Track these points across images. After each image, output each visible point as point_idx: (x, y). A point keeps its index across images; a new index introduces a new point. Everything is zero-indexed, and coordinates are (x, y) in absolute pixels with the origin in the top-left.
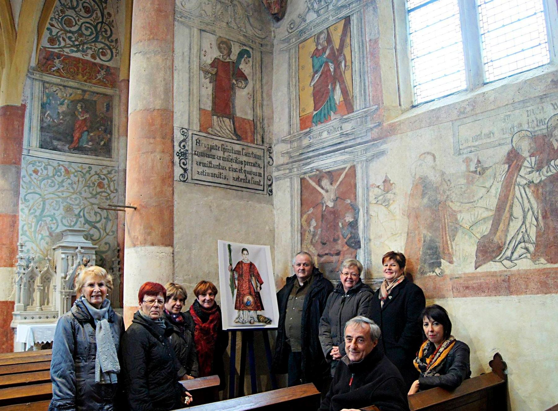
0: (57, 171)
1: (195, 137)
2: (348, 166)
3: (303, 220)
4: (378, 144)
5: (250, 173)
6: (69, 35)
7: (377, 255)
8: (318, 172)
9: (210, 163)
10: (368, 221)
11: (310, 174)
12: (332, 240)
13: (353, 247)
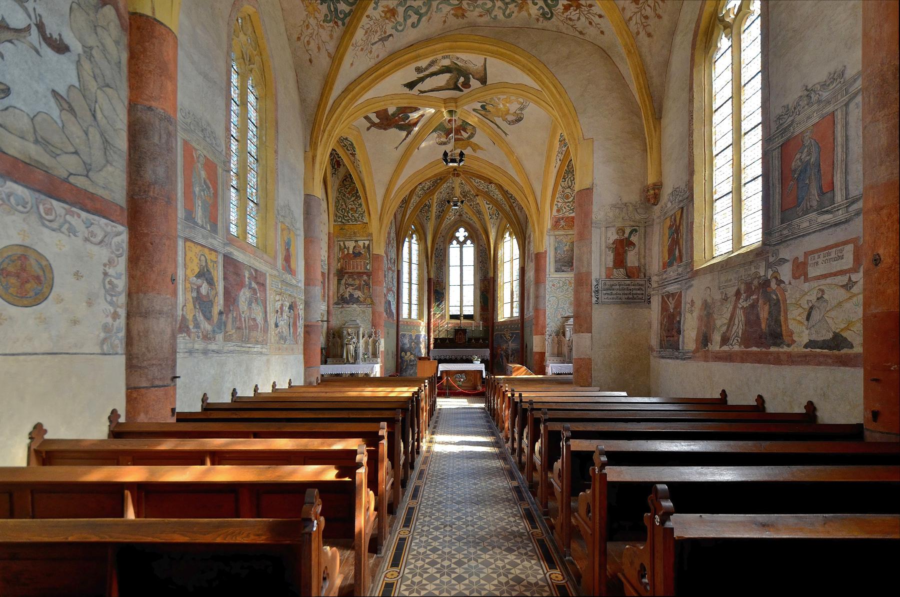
0: (564, 283)
1: (603, 282)
2: (679, 291)
5: (636, 294)
6: (567, 204)
9: (612, 293)
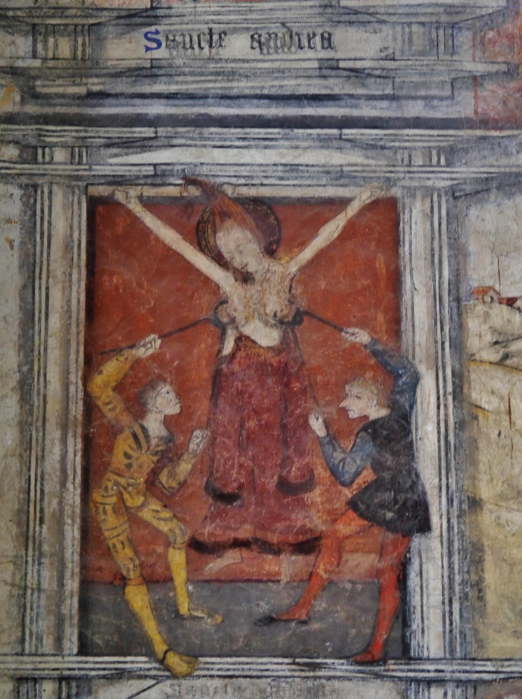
3: (98, 380)
4: (506, 142)
7: (512, 565)
8: (194, 191)
10: (461, 425)
11: (150, 192)
12: (271, 483)
13: (389, 525)
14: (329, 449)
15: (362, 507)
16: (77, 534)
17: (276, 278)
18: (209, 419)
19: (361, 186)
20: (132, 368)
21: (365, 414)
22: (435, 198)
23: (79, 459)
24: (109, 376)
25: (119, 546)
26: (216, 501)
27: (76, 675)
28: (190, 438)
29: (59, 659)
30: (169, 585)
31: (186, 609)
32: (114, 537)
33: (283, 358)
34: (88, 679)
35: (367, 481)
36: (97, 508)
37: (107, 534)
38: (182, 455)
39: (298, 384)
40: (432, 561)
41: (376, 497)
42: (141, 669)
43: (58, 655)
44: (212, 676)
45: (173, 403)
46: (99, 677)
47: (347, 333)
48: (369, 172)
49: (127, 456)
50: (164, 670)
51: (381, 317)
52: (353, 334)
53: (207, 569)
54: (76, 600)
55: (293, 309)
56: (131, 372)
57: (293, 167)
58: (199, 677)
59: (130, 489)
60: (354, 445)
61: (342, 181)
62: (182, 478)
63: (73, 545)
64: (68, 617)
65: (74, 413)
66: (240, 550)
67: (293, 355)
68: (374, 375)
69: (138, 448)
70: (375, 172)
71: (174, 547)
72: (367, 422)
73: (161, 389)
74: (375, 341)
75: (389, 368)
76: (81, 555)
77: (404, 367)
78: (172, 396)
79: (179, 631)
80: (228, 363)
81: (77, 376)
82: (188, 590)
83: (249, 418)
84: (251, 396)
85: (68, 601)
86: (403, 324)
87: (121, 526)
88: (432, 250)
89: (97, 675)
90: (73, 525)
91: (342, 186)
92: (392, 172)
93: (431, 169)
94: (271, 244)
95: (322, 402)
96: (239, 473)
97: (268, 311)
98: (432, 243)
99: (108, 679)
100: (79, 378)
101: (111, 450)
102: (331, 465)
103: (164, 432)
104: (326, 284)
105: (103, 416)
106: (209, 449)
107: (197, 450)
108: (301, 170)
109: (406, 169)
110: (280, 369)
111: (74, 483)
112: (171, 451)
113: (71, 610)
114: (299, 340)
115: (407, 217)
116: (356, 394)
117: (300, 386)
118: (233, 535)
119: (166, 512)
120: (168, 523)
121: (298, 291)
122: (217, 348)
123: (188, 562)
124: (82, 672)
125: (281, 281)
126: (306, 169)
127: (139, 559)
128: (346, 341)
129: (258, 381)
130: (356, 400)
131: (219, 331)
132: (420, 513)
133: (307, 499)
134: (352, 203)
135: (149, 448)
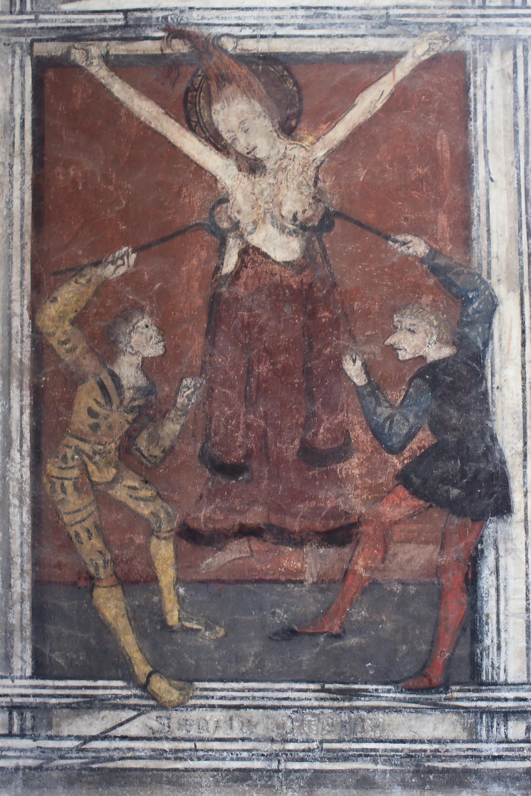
14: (371, 403)
15: (417, 481)
16: (27, 519)
17: (296, 167)
18: (204, 362)
19: (415, 36)
20: (96, 293)
21: (421, 353)
22: (520, 52)
23: (26, 417)
24: (65, 305)
25: (84, 535)
26: (214, 474)
27: (31, 703)
28: (179, 389)
29: (8, 682)
30: (152, 586)
31: (176, 618)
32: (76, 523)
33: (306, 277)
34: (46, 709)
35: (424, 446)
36: (53, 484)
37: (66, 519)
38: (168, 411)
39: (326, 314)
40: (513, 554)
41: (437, 468)
42: (116, 696)
43: (6, 678)
44: (212, 707)
45: (154, 340)
46: (61, 706)
47: (395, 241)
48: (426, 16)
49: (91, 413)
50: (147, 698)
51: (443, 220)
52: (404, 244)
53: (203, 565)
54: (27, 605)
55: (320, 209)
56: (95, 299)
57: (319, 11)
58: (194, 707)
59: (97, 458)
60: (405, 396)
61: (389, 30)
62: (167, 443)
63: (22, 534)
64: (18, 628)
65: (19, 356)
66: (249, 540)
67: (319, 273)
68: (434, 300)
69: (106, 403)
70: (434, 16)
71: (158, 537)
72: (423, 364)
73: (138, 322)
74: (434, 253)
75: (454, 290)
76: (33, 547)
77: (476, 289)
78: (152, 331)
79: (168, 648)
80: (230, 285)
81: (22, 306)
82: (178, 594)
83: (259, 362)
84: (262, 330)
85: (18, 607)
86: (474, 228)
87: (85, 507)
88: (516, 124)
89: (59, 704)
90: (21, 507)
91: (388, 36)
92: (458, 16)
93: (514, 11)
94: (288, 118)
95: (360, 338)
96: (246, 436)
97: (284, 213)
98: (515, 115)
99: (73, 708)
100: (25, 307)
101: (70, 405)
102: (373, 424)
103: (142, 382)
104: (367, 173)
105: (59, 359)
106: (204, 404)
107: (188, 405)
108: (330, 15)
109: (479, 12)
110: (302, 292)
111: (20, 451)
112: (152, 406)
113: (21, 620)
114: (329, 252)
115: (479, 79)
116: (408, 327)
117: (331, 316)
118: (238, 519)
119: (147, 489)
120: (150, 504)
121: (326, 184)
122: (214, 264)
123: (177, 556)
124: (39, 700)
125: (303, 171)
126: (336, 12)
127: (111, 552)
128: (395, 252)
129: (271, 308)
130: (409, 335)
131: (217, 240)
132: (496, 489)
133: (341, 470)
134: (403, 60)
135: (121, 402)
